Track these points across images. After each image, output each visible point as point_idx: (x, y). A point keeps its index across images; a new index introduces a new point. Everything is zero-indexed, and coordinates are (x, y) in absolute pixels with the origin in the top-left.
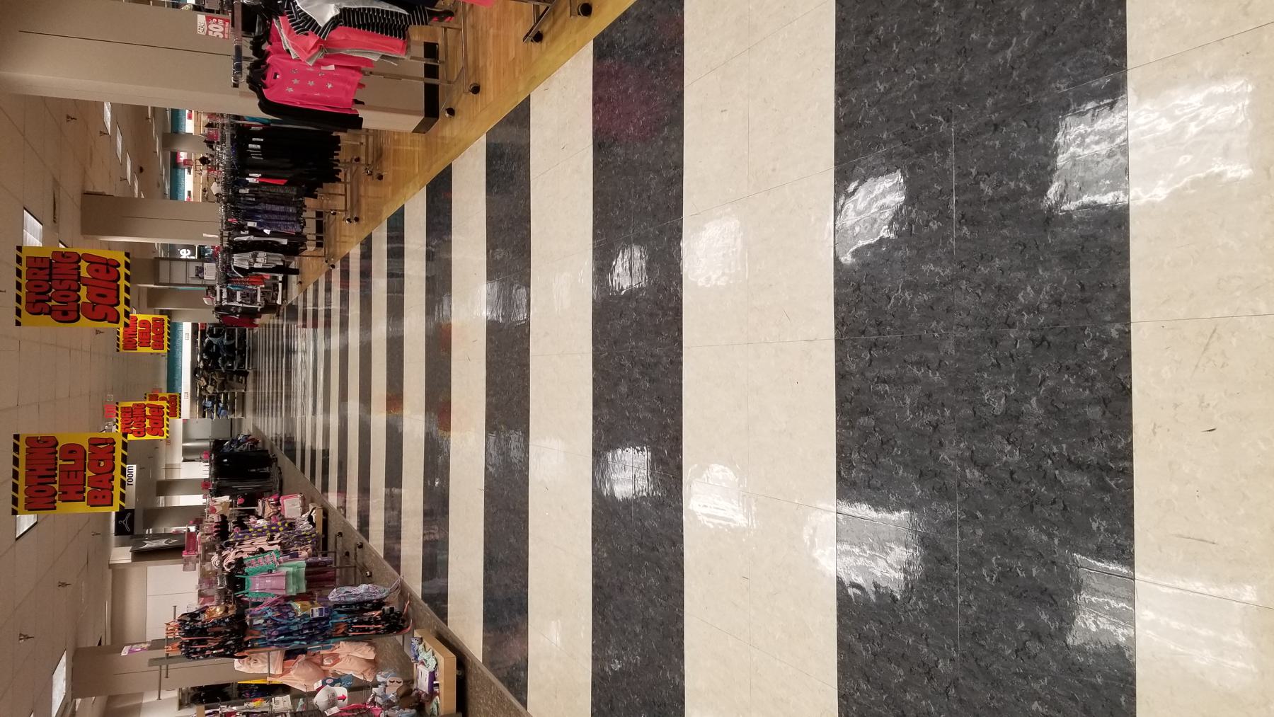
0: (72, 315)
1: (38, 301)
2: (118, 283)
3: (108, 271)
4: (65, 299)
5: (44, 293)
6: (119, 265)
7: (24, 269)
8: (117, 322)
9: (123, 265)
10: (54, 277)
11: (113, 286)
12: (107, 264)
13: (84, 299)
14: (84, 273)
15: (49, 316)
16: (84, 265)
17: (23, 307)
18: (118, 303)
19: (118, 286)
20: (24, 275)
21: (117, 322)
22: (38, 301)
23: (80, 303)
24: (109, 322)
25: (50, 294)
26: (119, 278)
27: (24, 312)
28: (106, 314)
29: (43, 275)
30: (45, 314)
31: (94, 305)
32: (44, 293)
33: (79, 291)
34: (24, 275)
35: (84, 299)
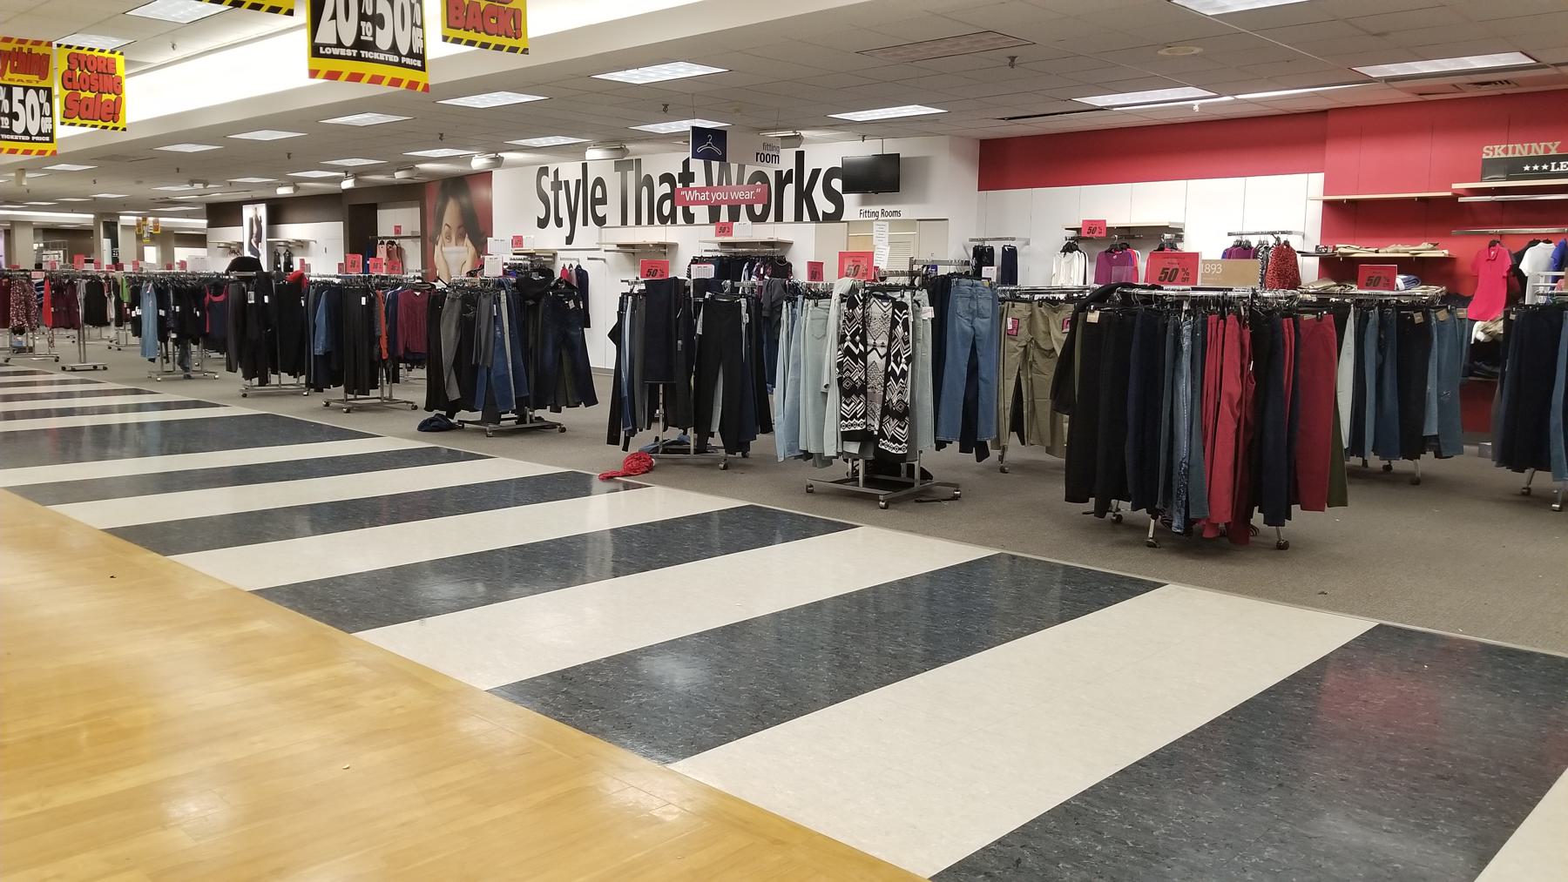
0: (68, 84)
1: (79, 62)
4: (82, 81)
5: (86, 67)
7: (106, 55)
10: (101, 75)
11: (97, 116)
13: (83, 95)
14: (105, 97)
15: (67, 68)
16: (113, 97)
17: (73, 50)
18: (81, 119)
20: (101, 54)
21: (64, 117)
22: (79, 62)
23: (80, 91)
25: (86, 71)
27: (69, 51)
29: (102, 68)
30: (69, 66)
31: (79, 101)
32: (86, 67)
33: (90, 91)
34: (101, 54)
35: (83, 95)
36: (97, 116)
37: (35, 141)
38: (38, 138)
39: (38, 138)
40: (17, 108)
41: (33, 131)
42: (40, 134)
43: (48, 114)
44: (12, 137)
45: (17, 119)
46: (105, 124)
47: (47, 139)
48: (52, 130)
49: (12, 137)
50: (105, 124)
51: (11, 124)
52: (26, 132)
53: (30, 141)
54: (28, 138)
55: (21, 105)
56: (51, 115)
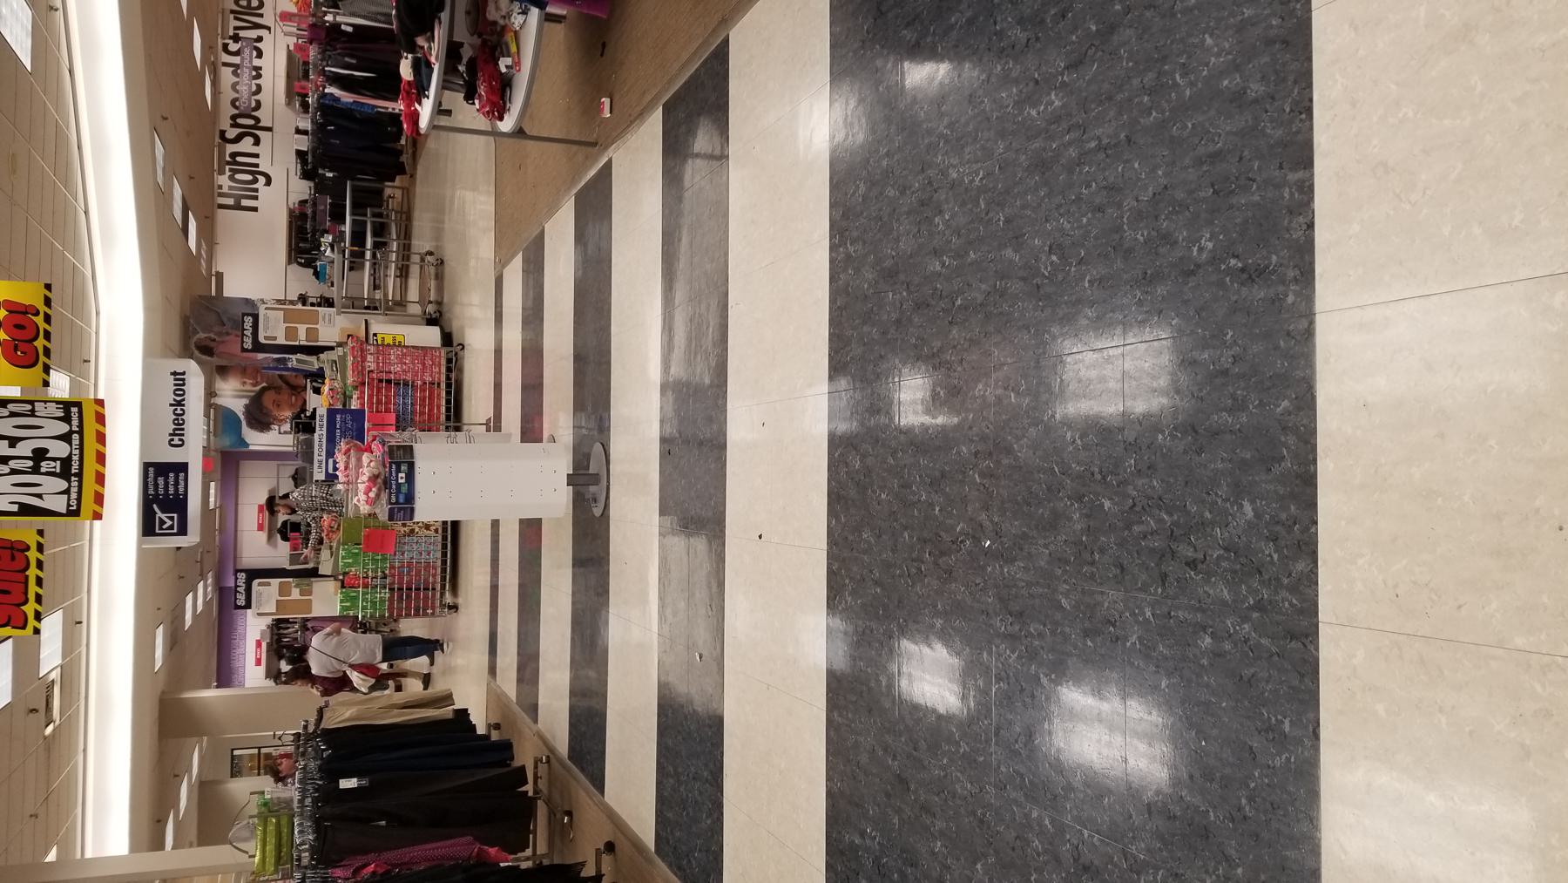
2: (27, 573)
3: (13, 558)
6: (28, 548)
8: (24, 627)
9: (34, 546)
12: (12, 548)
18: (26, 602)
19: (27, 577)
24: (13, 628)
26: (27, 567)
28: (10, 617)
36: (20, 577)
37: (81, 425)
38: (75, 422)
39: (75, 422)
40: (25, 449)
41: (63, 428)
42: (66, 419)
43: (29, 407)
44: (75, 458)
45: (46, 451)
46: (33, 564)
47: (74, 410)
48: (58, 402)
49: (75, 458)
50: (33, 564)
51: (54, 459)
52: (66, 438)
53: (81, 433)
54: (76, 437)
55: (20, 444)
56: (31, 403)
